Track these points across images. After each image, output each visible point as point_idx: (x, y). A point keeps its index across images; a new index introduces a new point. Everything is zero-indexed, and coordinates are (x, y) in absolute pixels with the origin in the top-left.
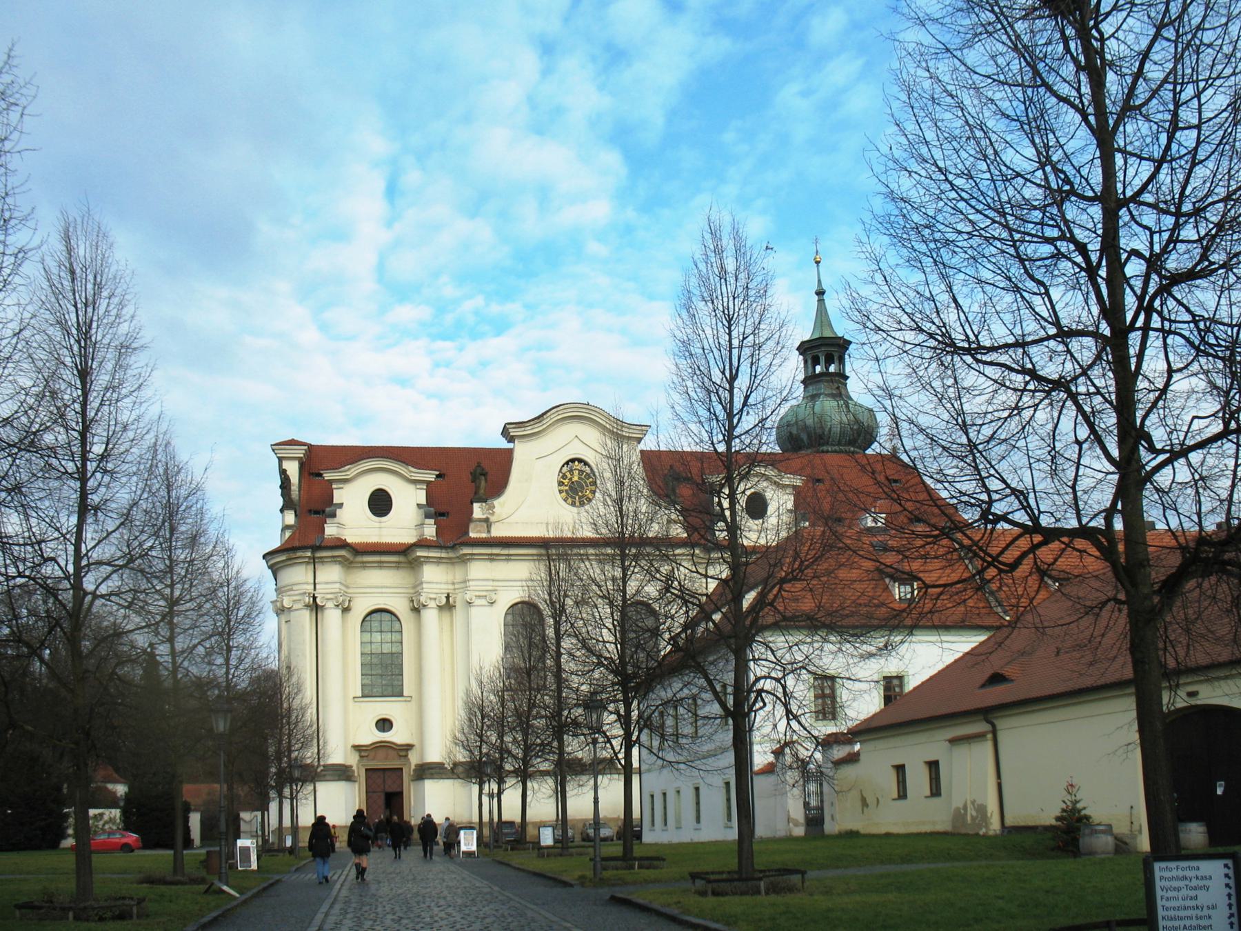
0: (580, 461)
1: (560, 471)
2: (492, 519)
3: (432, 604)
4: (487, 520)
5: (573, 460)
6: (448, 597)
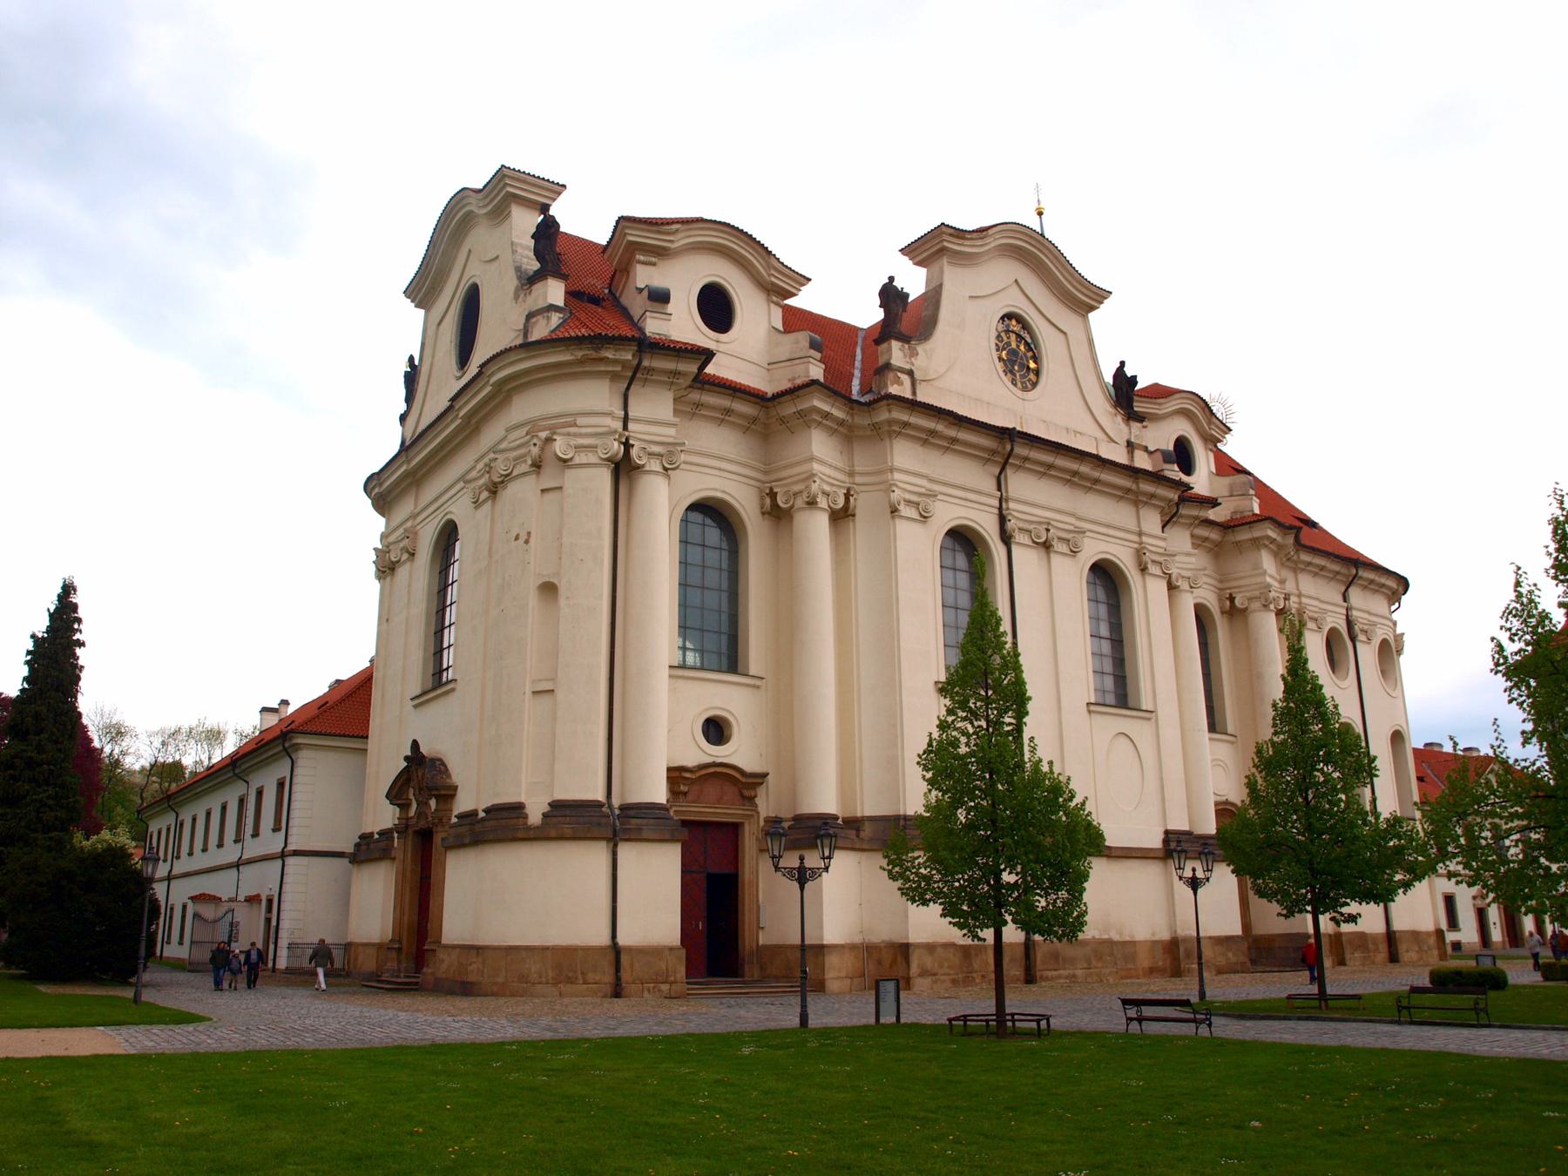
0: (1020, 319)
1: (997, 329)
2: (917, 375)
3: (823, 502)
4: (910, 373)
5: (1008, 316)
6: (847, 496)
